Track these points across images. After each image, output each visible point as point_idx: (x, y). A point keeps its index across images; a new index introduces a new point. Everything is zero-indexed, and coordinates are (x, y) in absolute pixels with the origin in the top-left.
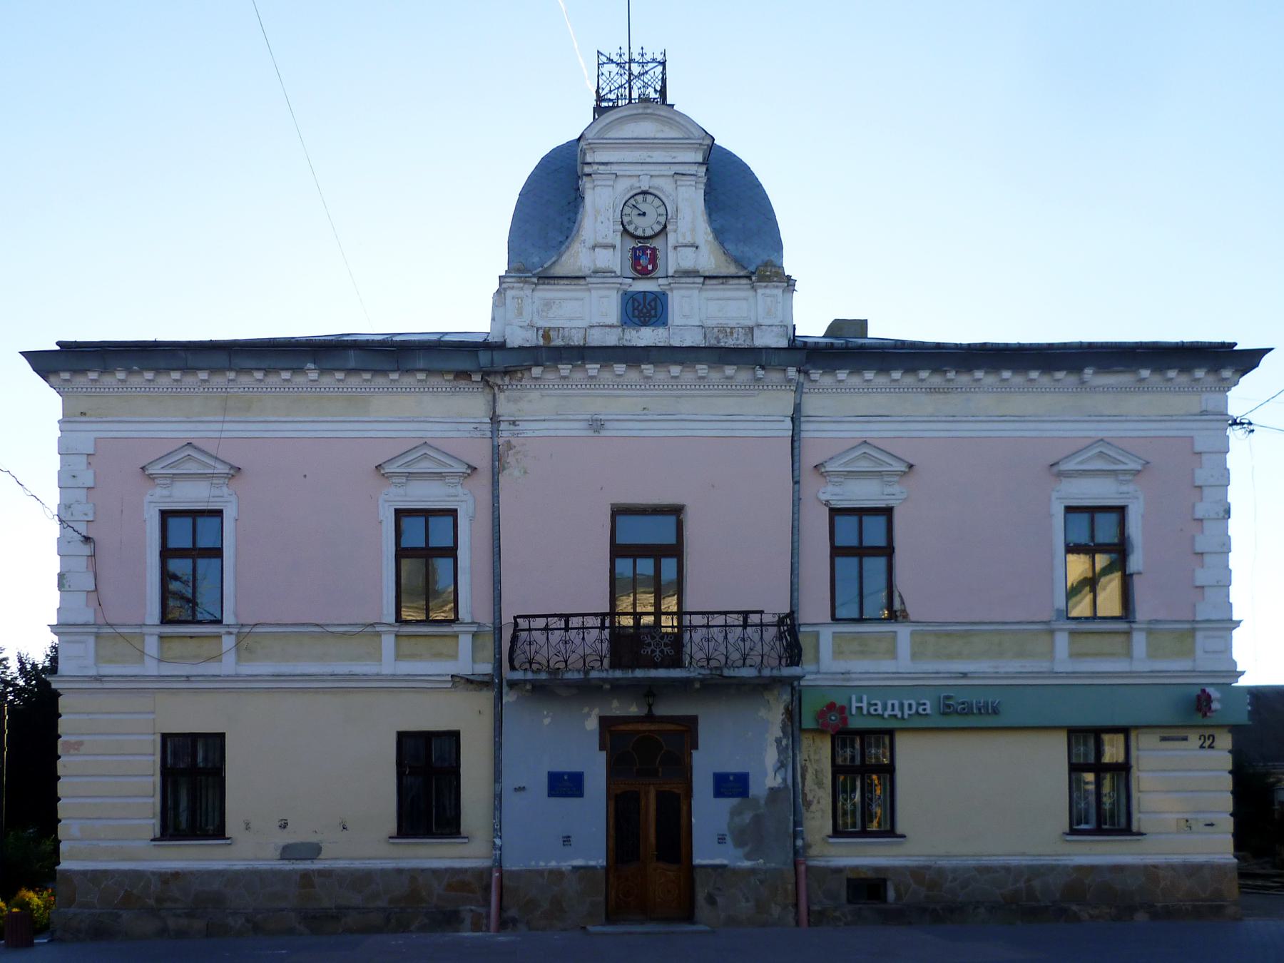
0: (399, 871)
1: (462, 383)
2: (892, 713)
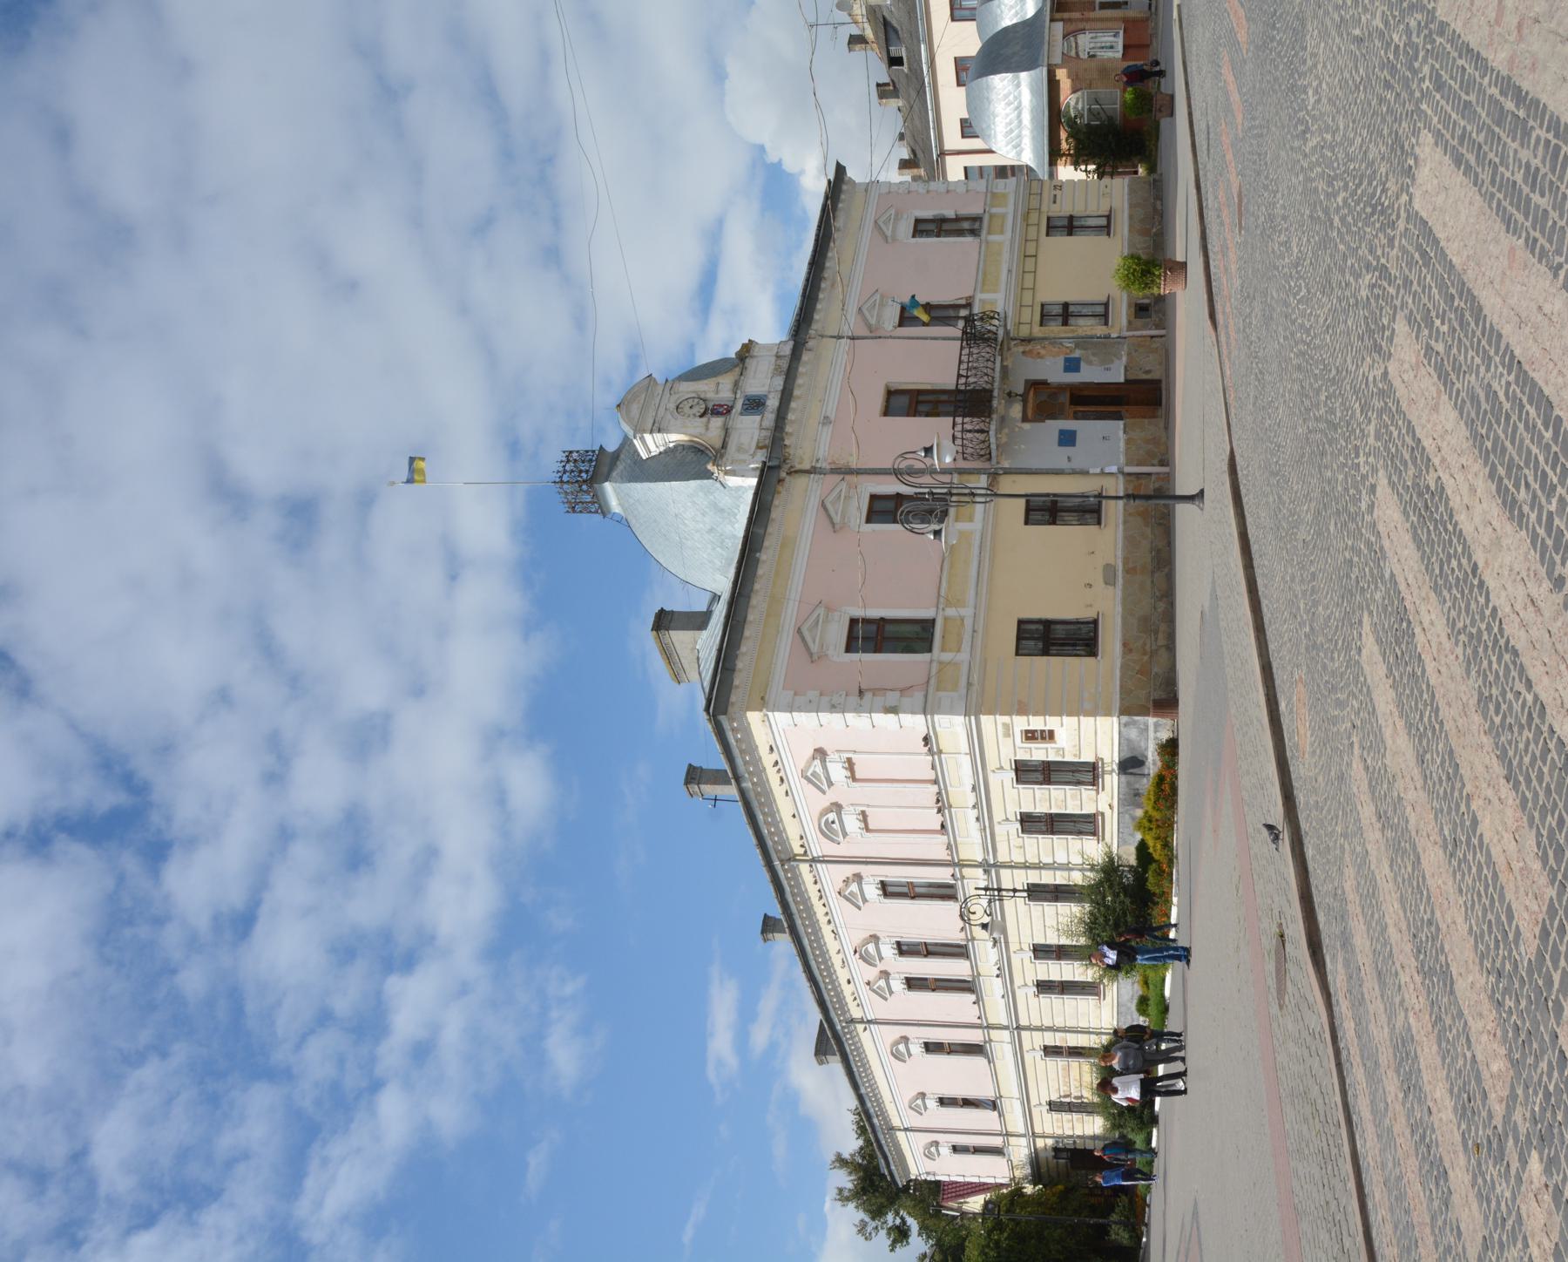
0: (1125, 522)
1: (786, 484)
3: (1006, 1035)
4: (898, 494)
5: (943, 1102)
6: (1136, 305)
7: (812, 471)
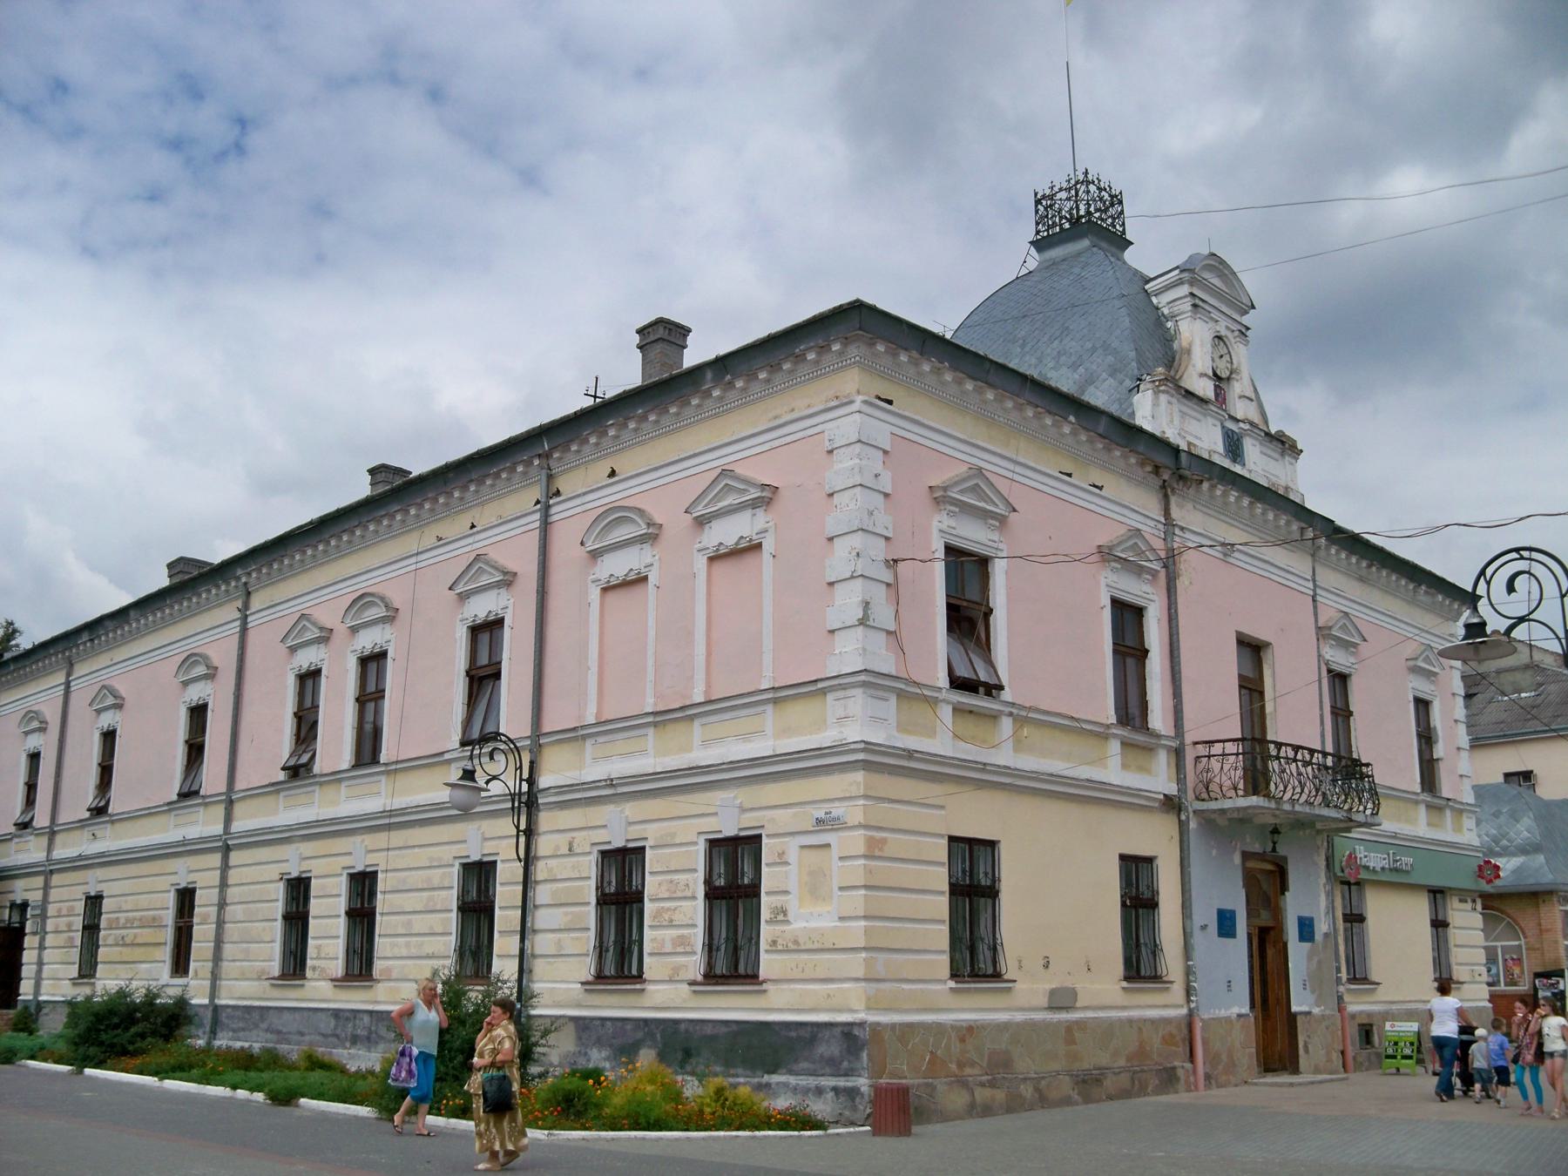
3: (218, 829)
4: (1147, 651)
5: (109, 737)
6: (1371, 1025)
7: (1169, 522)
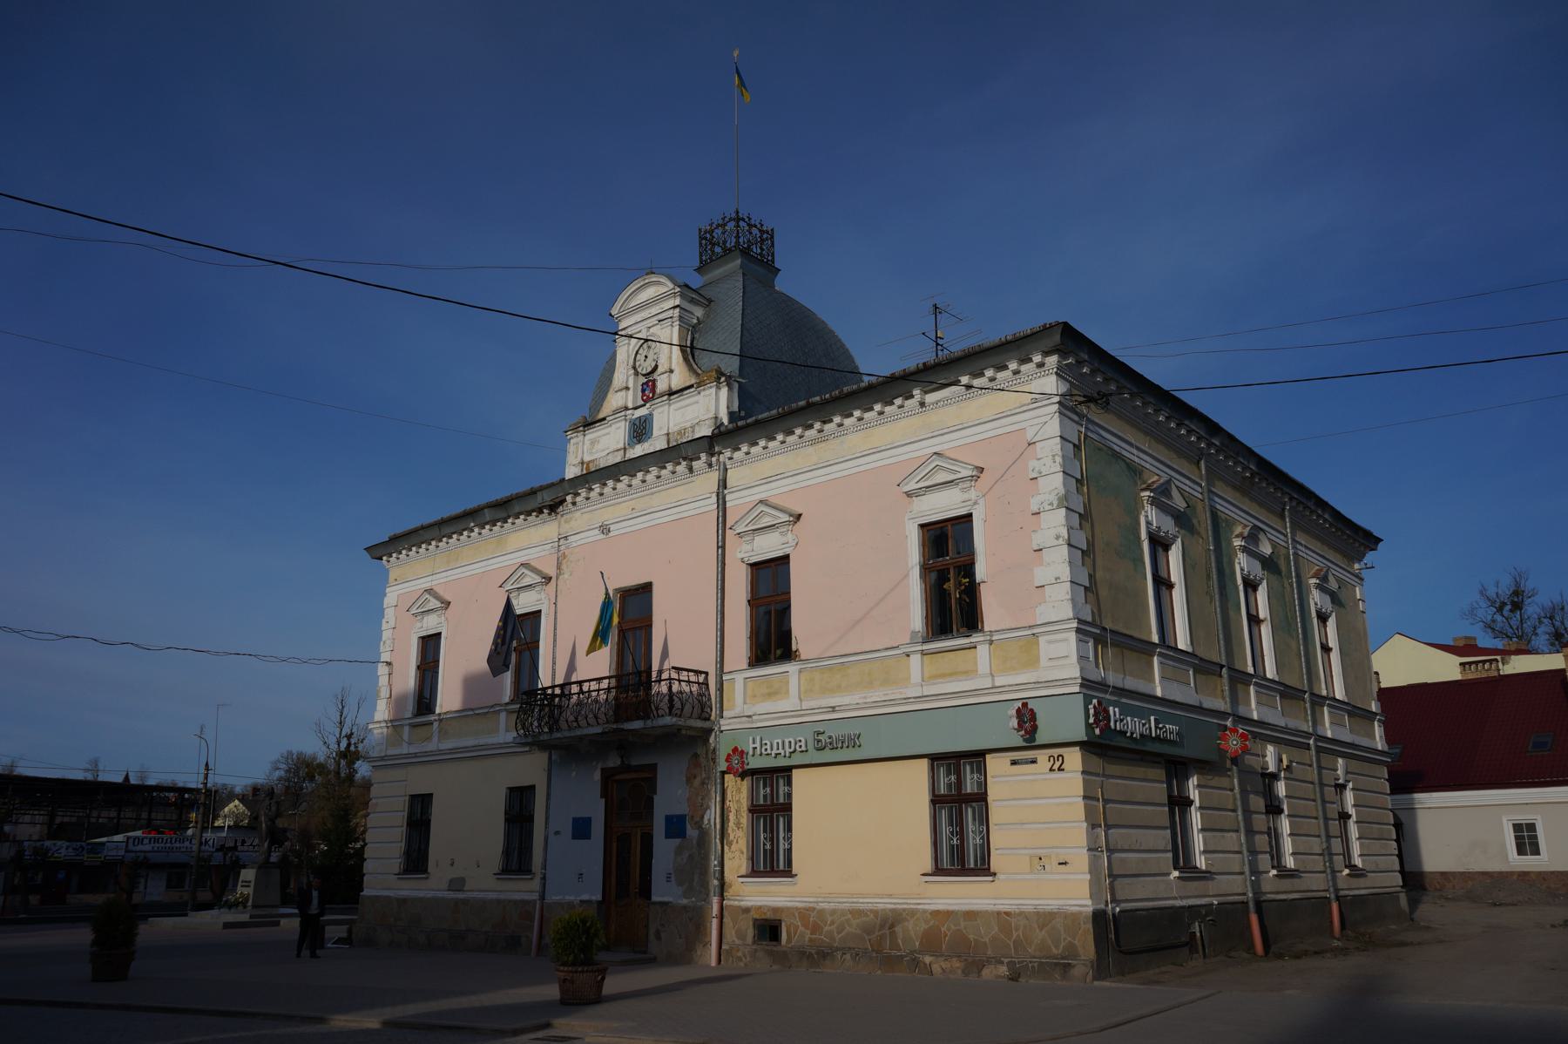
0: (499, 901)
2: (778, 752)
